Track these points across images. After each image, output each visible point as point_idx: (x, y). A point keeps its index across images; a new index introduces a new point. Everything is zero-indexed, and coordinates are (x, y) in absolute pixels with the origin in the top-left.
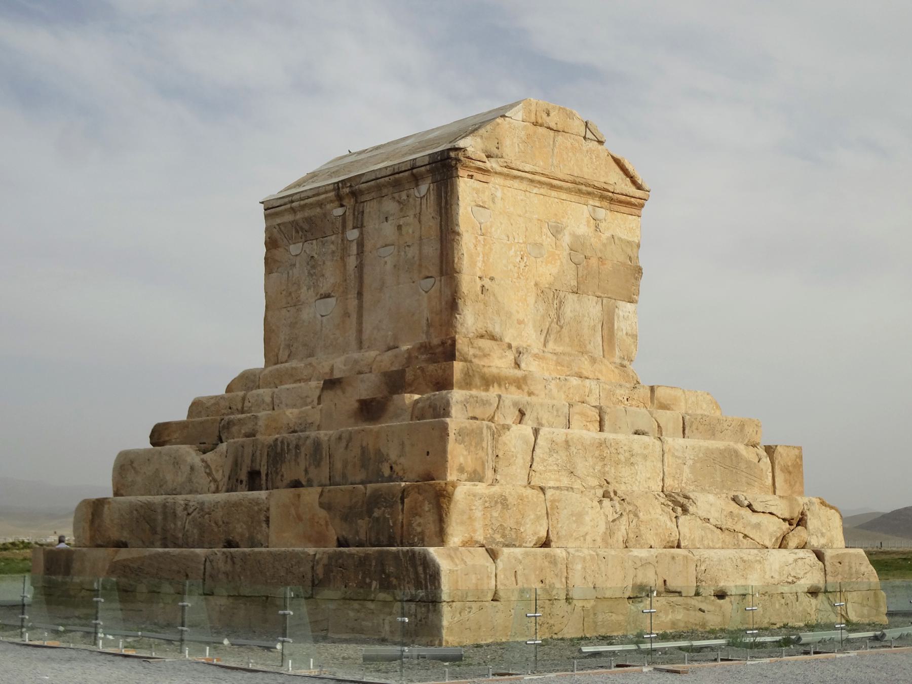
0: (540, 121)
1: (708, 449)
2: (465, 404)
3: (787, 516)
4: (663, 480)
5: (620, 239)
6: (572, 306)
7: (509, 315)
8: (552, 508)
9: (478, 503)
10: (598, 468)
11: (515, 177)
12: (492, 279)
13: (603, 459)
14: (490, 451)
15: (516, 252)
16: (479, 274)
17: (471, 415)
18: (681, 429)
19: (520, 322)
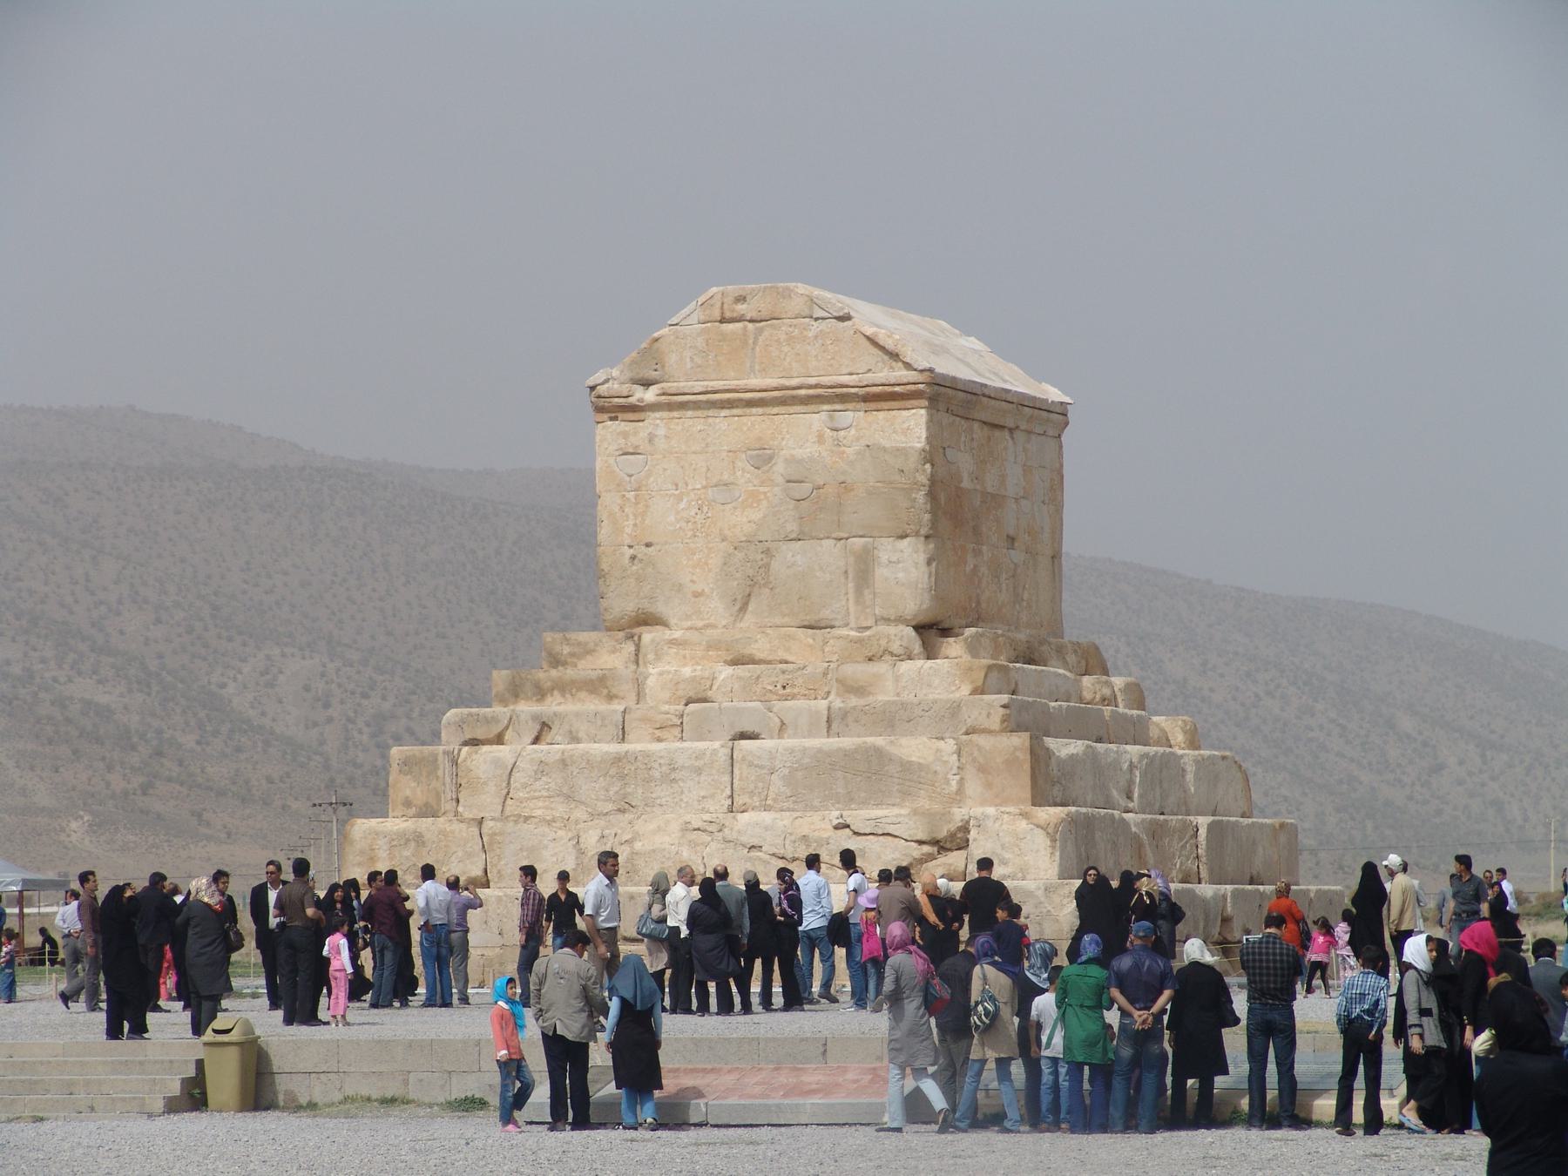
0: (728, 315)
1: (820, 750)
2: (460, 725)
3: (921, 836)
4: (732, 796)
5: (885, 450)
6: (793, 556)
7: (680, 588)
8: (491, 844)
9: (381, 842)
10: (613, 790)
11: (683, 406)
12: (648, 545)
13: (623, 777)
14: (448, 780)
15: (689, 502)
16: (628, 541)
17: (468, 736)
18: (824, 724)
19: (697, 595)
